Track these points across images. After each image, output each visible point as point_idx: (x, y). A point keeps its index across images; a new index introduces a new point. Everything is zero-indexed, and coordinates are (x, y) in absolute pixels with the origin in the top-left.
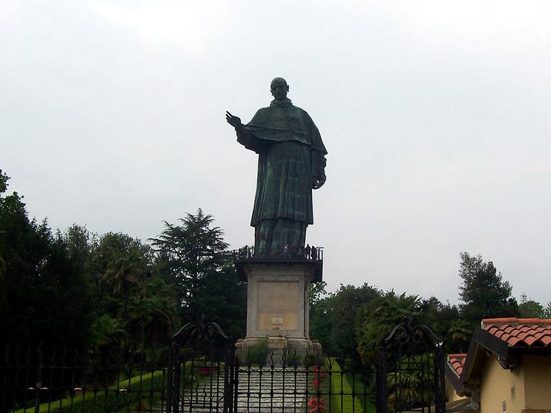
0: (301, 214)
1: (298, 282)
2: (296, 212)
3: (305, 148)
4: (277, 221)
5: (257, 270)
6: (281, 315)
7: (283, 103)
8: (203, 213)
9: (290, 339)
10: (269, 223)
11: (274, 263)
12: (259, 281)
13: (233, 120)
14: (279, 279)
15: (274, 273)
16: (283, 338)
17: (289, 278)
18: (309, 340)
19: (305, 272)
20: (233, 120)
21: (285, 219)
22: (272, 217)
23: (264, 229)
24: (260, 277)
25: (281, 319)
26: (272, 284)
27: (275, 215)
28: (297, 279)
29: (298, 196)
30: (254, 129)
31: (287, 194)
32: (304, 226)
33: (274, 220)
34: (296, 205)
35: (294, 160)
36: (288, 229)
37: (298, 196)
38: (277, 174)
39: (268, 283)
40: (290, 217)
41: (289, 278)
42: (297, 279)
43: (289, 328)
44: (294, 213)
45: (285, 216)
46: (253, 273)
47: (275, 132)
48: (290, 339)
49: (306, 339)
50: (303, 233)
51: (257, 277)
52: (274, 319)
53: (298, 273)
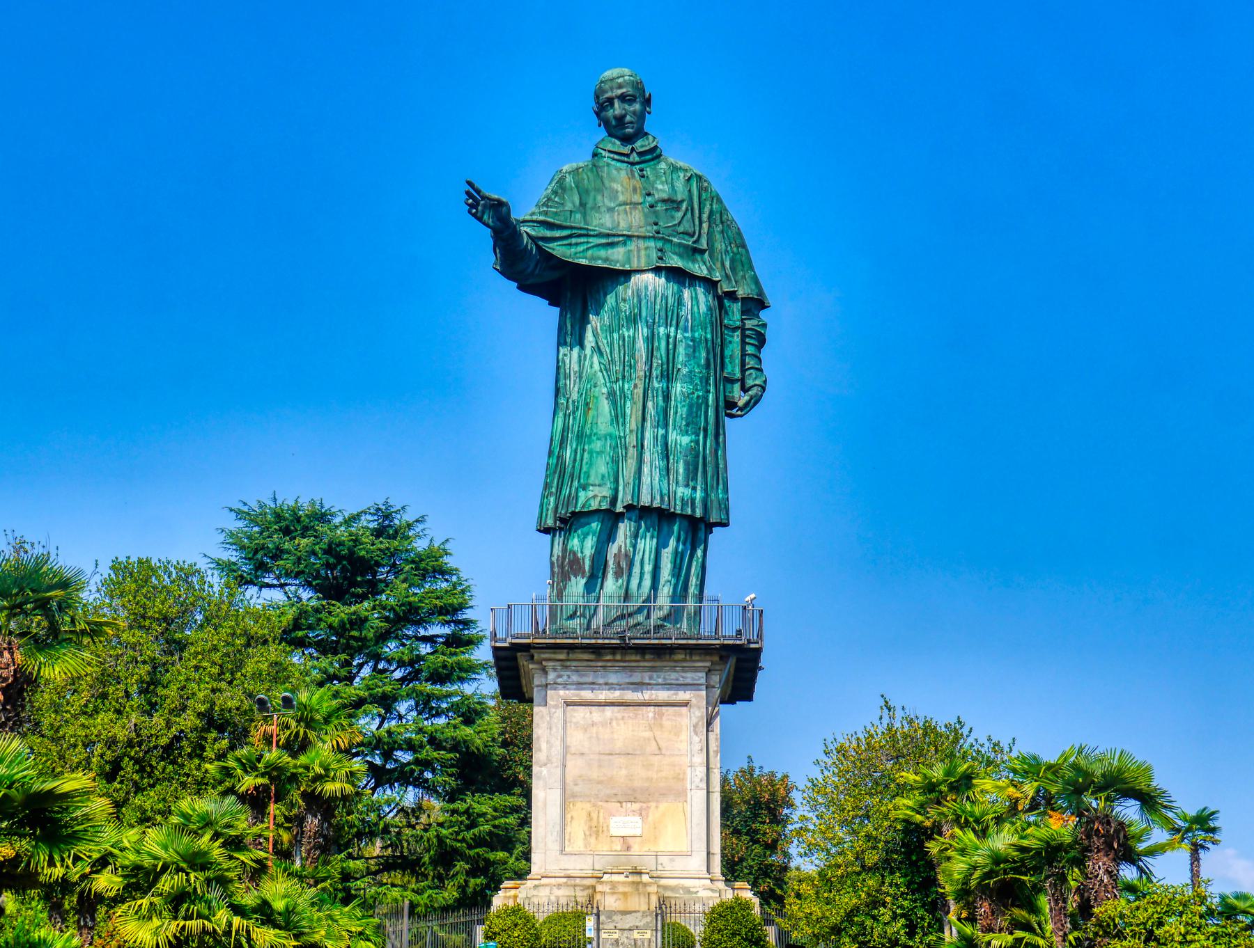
4: (619, 517)
5: (567, 667)
6: (636, 806)
7: (633, 150)
8: (756, 765)
9: (663, 882)
11: (613, 649)
12: (568, 704)
15: (613, 678)
16: (645, 878)
18: (721, 885)
19: (709, 672)
22: (605, 506)
26: (609, 711)
27: (614, 500)
30: (549, 233)
32: (701, 535)
37: (686, 440)
40: (656, 504)
41: (663, 695)
42: (683, 696)
43: (661, 847)
45: (645, 500)
46: (552, 676)
47: (612, 239)
48: (663, 882)
49: (712, 880)
53: (690, 677)
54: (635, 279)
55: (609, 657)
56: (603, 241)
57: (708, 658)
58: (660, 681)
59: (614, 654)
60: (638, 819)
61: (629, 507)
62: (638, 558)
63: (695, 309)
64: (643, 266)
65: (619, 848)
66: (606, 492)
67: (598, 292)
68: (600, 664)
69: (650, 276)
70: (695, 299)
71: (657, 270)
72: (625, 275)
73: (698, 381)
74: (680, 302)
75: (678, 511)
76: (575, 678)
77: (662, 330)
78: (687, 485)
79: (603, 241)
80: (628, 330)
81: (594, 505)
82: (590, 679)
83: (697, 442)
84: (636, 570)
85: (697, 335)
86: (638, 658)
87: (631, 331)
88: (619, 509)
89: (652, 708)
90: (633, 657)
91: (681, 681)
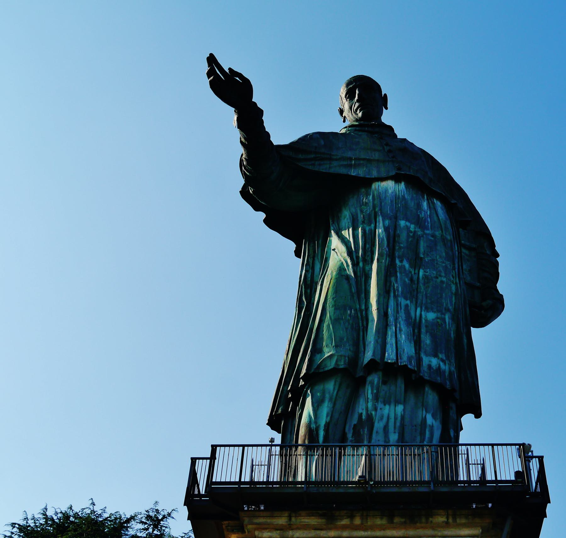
0: (445, 367)
2: (426, 360)
3: (438, 204)
10: (330, 386)
21: (391, 371)
23: (316, 407)
29: (431, 316)
31: (392, 303)
33: (352, 376)
34: (427, 340)
35: (412, 227)
36: (400, 408)
37: (431, 316)
38: (360, 258)
40: (404, 361)
44: (419, 361)
50: (452, 433)
54: (375, 185)
55: (345, 522)
56: (345, 163)
57: (477, 520)
59: (352, 517)
61: (373, 366)
62: (378, 425)
63: (435, 215)
64: (384, 175)
66: (347, 350)
67: (340, 211)
69: (390, 185)
70: (432, 207)
71: (397, 179)
72: (367, 182)
73: (441, 269)
74: (419, 206)
75: (427, 377)
77: (402, 223)
78: (436, 356)
79: (345, 163)
80: (370, 223)
81: (331, 365)
83: (444, 320)
84: (378, 438)
85: (438, 233)
86: (384, 522)
87: (373, 226)
88: (360, 373)
90: (378, 522)
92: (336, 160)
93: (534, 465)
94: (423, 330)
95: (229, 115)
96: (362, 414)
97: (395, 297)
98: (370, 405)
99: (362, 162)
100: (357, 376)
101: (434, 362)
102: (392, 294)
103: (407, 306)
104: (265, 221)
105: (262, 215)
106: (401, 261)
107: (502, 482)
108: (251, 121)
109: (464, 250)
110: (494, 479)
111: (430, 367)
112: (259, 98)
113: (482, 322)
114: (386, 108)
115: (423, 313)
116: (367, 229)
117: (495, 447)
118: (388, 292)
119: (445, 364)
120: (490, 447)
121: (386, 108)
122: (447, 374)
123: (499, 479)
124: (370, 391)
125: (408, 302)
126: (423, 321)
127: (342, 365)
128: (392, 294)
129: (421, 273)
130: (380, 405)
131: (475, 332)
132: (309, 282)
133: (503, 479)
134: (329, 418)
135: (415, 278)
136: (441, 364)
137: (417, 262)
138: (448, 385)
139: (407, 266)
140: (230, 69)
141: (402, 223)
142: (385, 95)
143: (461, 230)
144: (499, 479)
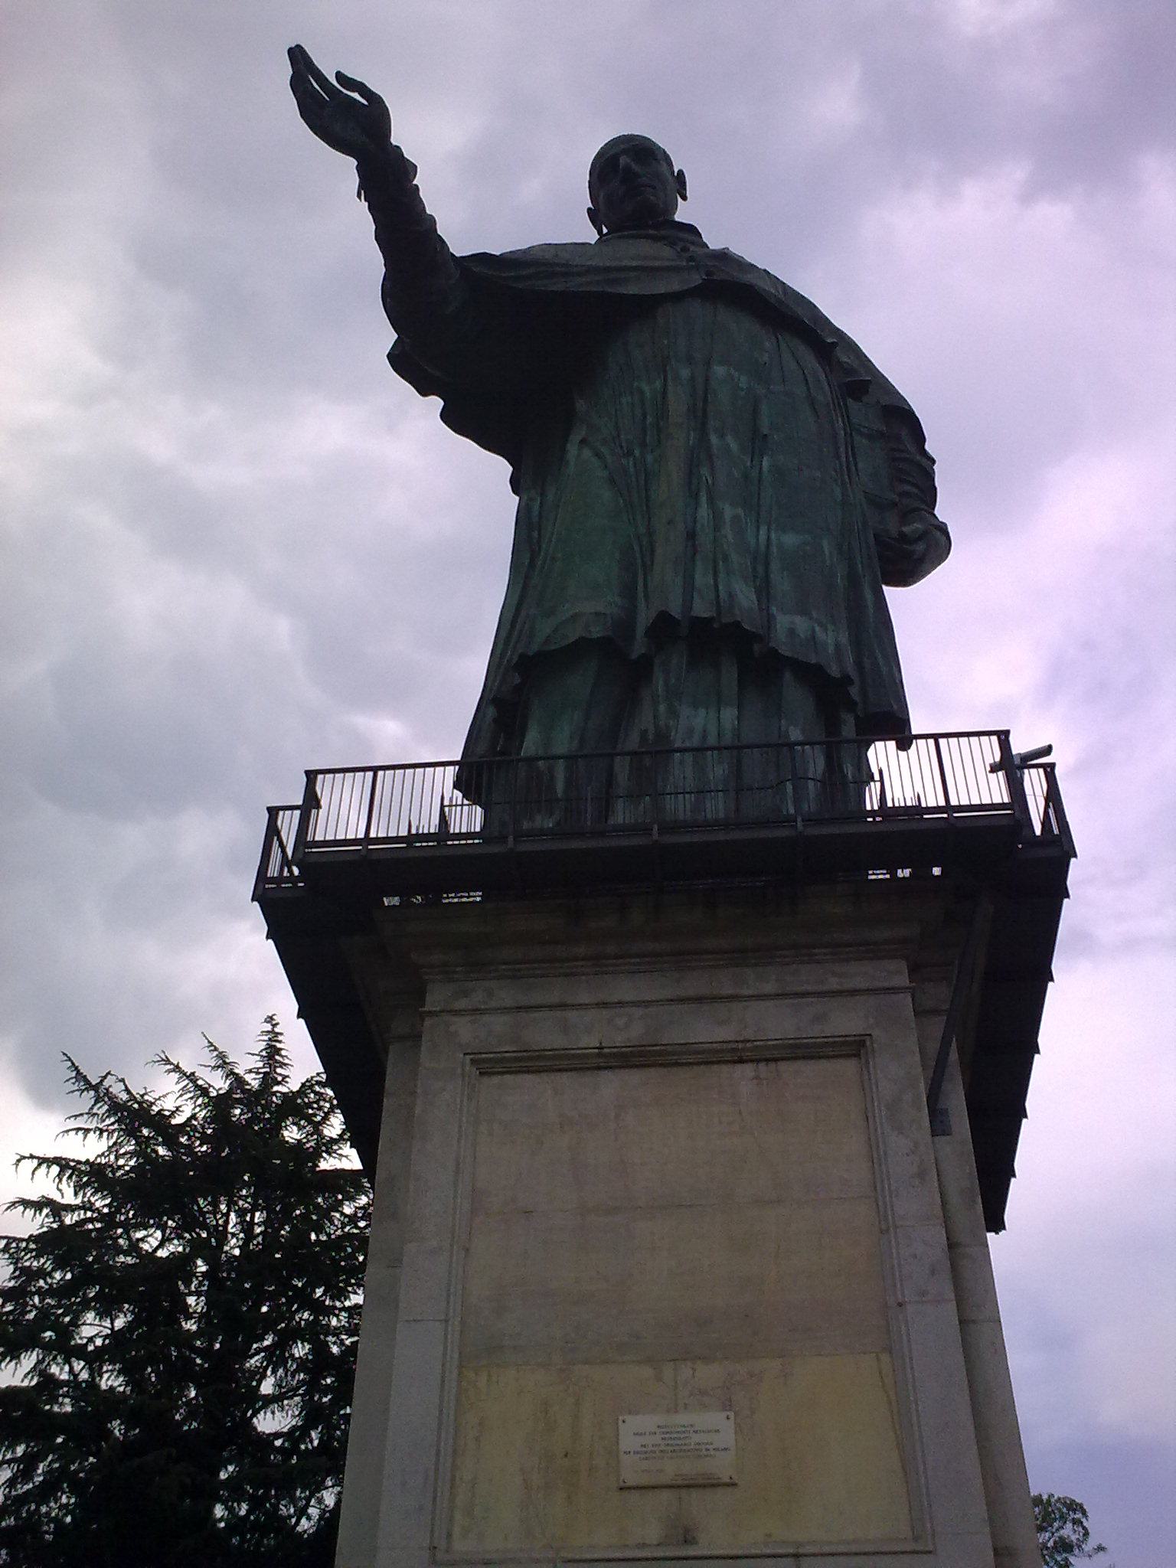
1: (855, 1048)
6: (709, 1374)
13: (345, 117)
14: (676, 1036)
17: (777, 1023)
20: (345, 117)
24: (499, 1023)
25: (715, 1428)
26: (611, 1085)
28: (845, 1021)
31: (704, 511)
34: (782, 583)
35: (744, 381)
37: (790, 540)
39: (564, 1079)
51: (465, 1030)
52: (637, 1430)
53: (860, 974)
58: (769, 988)
60: (716, 1419)
65: (653, 1533)
68: (581, 950)
75: (785, 651)
76: (506, 995)
77: (719, 371)
78: (804, 612)
82: (554, 997)
87: (658, 384)
89: (748, 1069)
91: (833, 983)
92: (579, 274)
93: (1034, 783)
94: (775, 566)
95: (343, 171)
96: (646, 731)
97: (711, 500)
98: (662, 708)
99: (632, 274)
100: (634, 656)
101: (801, 624)
102: (704, 499)
103: (736, 518)
104: (445, 416)
105: (436, 403)
106: (722, 436)
107: (960, 808)
108: (389, 185)
109: (857, 438)
110: (942, 803)
111: (792, 632)
112: (403, 135)
113: (908, 571)
114: (684, 198)
115: (773, 536)
116: (646, 389)
117: (942, 742)
118: (696, 496)
119: (826, 630)
120: (931, 742)
121: (684, 198)
122: (831, 649)
123: (954, 802)
124: (661, 682)
125: (740, 511)
126: (774, 549)
127: (596, 632)
128: (704, 499)
129: (765, 463)
130: (685, 711)
131: (892, 594)
132: (535, 520)
133: (965, 802)
134: (575, 743)
135: (754, 473)
136: (817, 629)
137: (757, 442)
138: (834, 671)
139: (734, 446)
140: (339, 76)
141: (719, 371)
142: (681, 172)
143: (850, 401)
144: (954, 802)
